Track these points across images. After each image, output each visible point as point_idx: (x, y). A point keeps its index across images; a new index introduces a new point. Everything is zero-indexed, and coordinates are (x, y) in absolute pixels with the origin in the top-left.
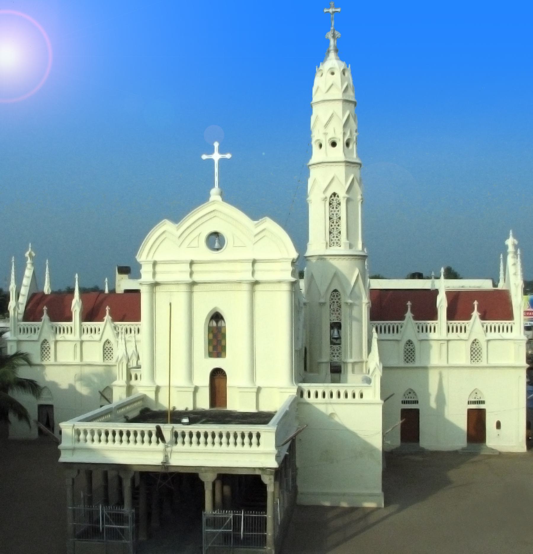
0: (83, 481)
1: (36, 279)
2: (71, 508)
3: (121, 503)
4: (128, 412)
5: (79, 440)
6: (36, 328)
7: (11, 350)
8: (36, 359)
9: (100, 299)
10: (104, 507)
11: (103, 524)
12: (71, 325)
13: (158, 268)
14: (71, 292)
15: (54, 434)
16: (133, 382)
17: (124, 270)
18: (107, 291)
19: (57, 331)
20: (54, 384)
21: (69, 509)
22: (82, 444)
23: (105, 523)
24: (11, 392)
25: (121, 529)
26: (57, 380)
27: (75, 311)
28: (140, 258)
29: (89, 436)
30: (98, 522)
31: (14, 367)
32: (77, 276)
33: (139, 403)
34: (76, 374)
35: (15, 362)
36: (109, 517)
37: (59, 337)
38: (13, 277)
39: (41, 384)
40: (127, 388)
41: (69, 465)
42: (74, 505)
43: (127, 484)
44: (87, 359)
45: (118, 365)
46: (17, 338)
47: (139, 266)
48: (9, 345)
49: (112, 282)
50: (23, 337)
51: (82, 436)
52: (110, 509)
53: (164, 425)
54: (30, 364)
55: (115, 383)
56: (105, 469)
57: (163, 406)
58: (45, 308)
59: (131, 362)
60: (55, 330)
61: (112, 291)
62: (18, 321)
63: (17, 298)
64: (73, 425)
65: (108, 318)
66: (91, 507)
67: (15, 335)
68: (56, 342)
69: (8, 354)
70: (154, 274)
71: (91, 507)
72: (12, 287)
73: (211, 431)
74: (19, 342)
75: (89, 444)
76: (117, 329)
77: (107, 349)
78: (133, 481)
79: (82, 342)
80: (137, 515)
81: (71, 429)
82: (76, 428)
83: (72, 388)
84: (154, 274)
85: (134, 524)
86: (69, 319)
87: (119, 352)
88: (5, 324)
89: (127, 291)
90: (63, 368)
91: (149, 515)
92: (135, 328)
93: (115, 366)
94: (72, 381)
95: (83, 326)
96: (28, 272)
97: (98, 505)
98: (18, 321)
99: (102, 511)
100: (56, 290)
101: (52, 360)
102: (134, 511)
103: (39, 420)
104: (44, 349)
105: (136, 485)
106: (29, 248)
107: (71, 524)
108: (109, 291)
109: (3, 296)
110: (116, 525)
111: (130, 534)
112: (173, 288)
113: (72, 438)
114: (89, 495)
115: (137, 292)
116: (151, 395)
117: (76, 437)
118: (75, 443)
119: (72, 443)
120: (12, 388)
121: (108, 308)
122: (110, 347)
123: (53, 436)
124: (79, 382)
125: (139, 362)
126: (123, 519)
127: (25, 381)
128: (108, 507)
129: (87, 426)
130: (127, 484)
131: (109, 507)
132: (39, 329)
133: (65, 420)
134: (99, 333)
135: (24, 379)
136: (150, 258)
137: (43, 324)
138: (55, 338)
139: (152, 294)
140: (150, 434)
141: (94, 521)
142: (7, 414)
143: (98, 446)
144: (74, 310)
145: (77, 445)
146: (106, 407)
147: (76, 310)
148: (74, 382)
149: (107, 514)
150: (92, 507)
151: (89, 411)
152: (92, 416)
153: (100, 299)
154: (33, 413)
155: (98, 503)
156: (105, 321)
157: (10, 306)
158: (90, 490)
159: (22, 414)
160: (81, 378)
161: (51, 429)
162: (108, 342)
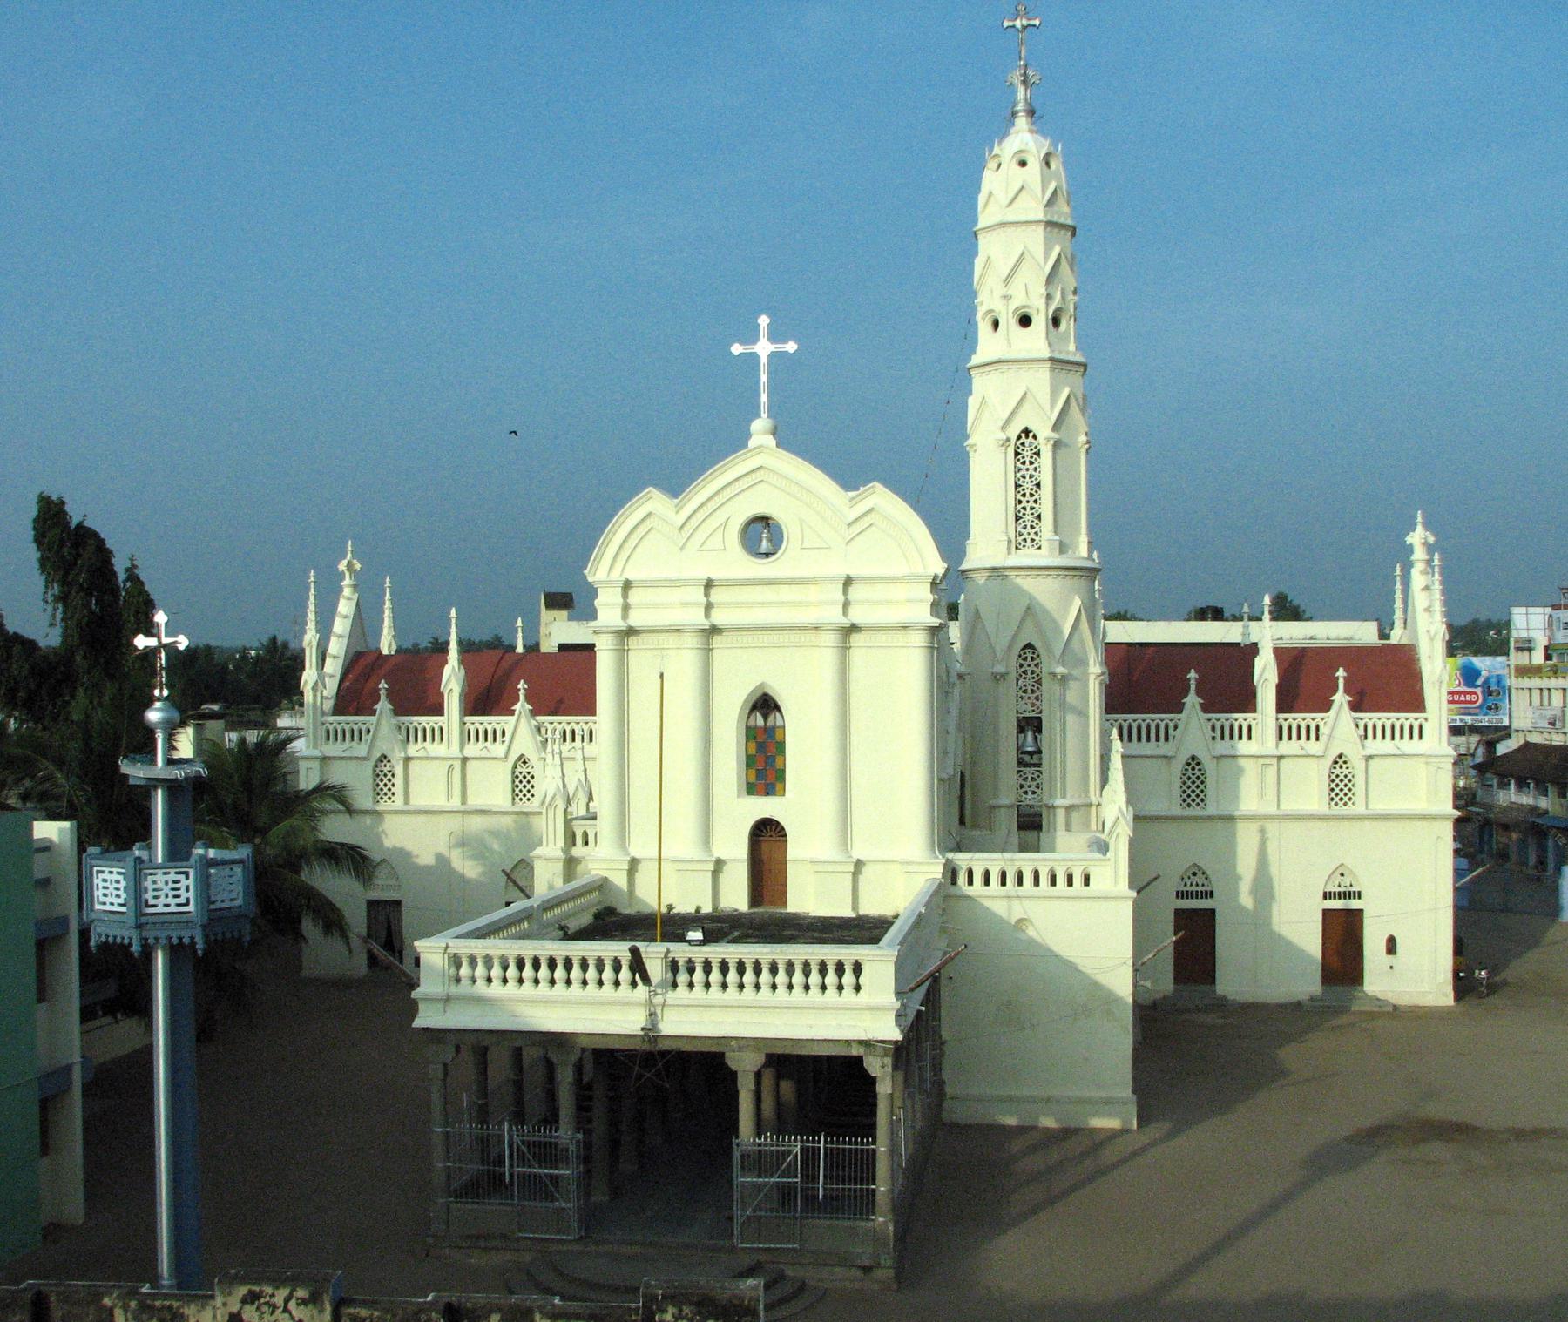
0: (467, 1070)
1: (364, 622)
2: (440, 1130)
3: (552, 1119)
4: (568, 916)
5: (458, 980)
6: (364, 728)
7: (307, 780)
8: (362, 800)
9: (504, 664)
10: (514, 1128)
11: (511, 1166)
12: (440, 724)
13: (635, 596)
14: (441, 648)
15: (401, 962)
16: (578, 851)
17: (559, 601)
18: (520, 649)
19: (409, 736)
20: (404, 854)
21: (436, 1132)
22: (465, 988)
23: (515, 1164)
24: (306, 872)
25: (551, 1176)
26: (409, 845)
27: (449, 693)
28: (595, 574)
29: (480, 971)
30: (501, 1162)
31: (313, 817)
32: (453, 613)
33: (594, 896)
34: (452, 833)
35: (315, 804)
36: (525, 1150)
37: (412, 750)
38: (311, 616)
39: (376, 857)
40: (564, 862)
41: (436, 1035)
42: (446, 1124)
43: (565, 1077)
44: (474, 801)
45: (544, 811)
46: (321, 751)
47: (592, 592)
48: (303, 766)
49: (533, 627)
50: (332, 749)
51: (465, 971)
52: (529, 1132)
53: (648, 946)
54: (350, 811)
55: (538, 851)
56: (517, 1044)
57: (646, 904)
58: (383, 685)
59: (574, 805)
60: (405, 735)
61: (532, 648)
62: (323, 714)
63: (320, 663)
64: (444, 945)
65: (522, 706)
66: (485, 1127)
67: (315, 746)
68: (408, 759)
69: (301, 788)
70: (626, 608)
71: (485, 1127)
72: (310, 637)
73: (769, 958)
74: (325, 759)
75: (481, 988)
76: (543, 730)
77: (521, 777)
78: (579, 1068)
79: (465, 760)
80: (588, 1145)
81: (441, 955)
82: (451, 951)
83: (442, 860)
84: (626, 608)
85: (582, 1166)
86: (438, 710)
87: (547, 783)
88: (294, 722)
89: (562, 647)
90: (422, 818)
91: (614, 1145)
92: (583, 731)
93: (540, 813)
94: (442, 848)
95: (468, 725)
96: (346, 607)
97: (500, 1123)
98: (323, 714)
99: (511, 1137)
100: (408, 645)
101: (398, 802)
102: (580, 1136)
103: (369, 936)
104: (382, 776)
105: (586, 1079)
106: (347, 554)
107: (440, 1165)
108: (525, 646)
109: (290, 659)
110: (540, 1167)
111: (573, 1188)
112: (671, 640)
113: (444, 975)
114: (480, 1102)
115: (589, 648)
116: (620, 880)
117: (453, 971)
118: (449, 985)
119: (444, 985)
120: (308, 863)
121: (522, 685)
122: (529, 773)
123: (401, 970)
124: (460, 850)
125: (591, 804)
126: (556, 1155)
127: (339, 847)
128: (522, 1127)
129: (476, 947)
130: (565, 1077)
131: (525, 1127)
132: (369, 731)
133: (428, 934)
134: (503, 742)
135: (336, 843)
136: (617, 576)
137: (379, 720)
138: (406, 753)
139: (622, 653)
140: (617, 967)
141: (492, 1158)
142: (299, 922)
143: (502, 992)
144: (447, 691)
145: (454, 990)
146: (517, 906)
147: (451, 690)
148: (447, 849)
149: (520, 1143)
150: (488, 1127)
151: (481, 914)
152: (488, 925)
153: (504, 664)
154: (357, 919)
155: (500, 1119)
156: (517, 713)
157: (306, 682)
158: (483, 1091)
159: (332, 920)
160: (463, 842)
161: (397, 954)
162: (522, 760)
